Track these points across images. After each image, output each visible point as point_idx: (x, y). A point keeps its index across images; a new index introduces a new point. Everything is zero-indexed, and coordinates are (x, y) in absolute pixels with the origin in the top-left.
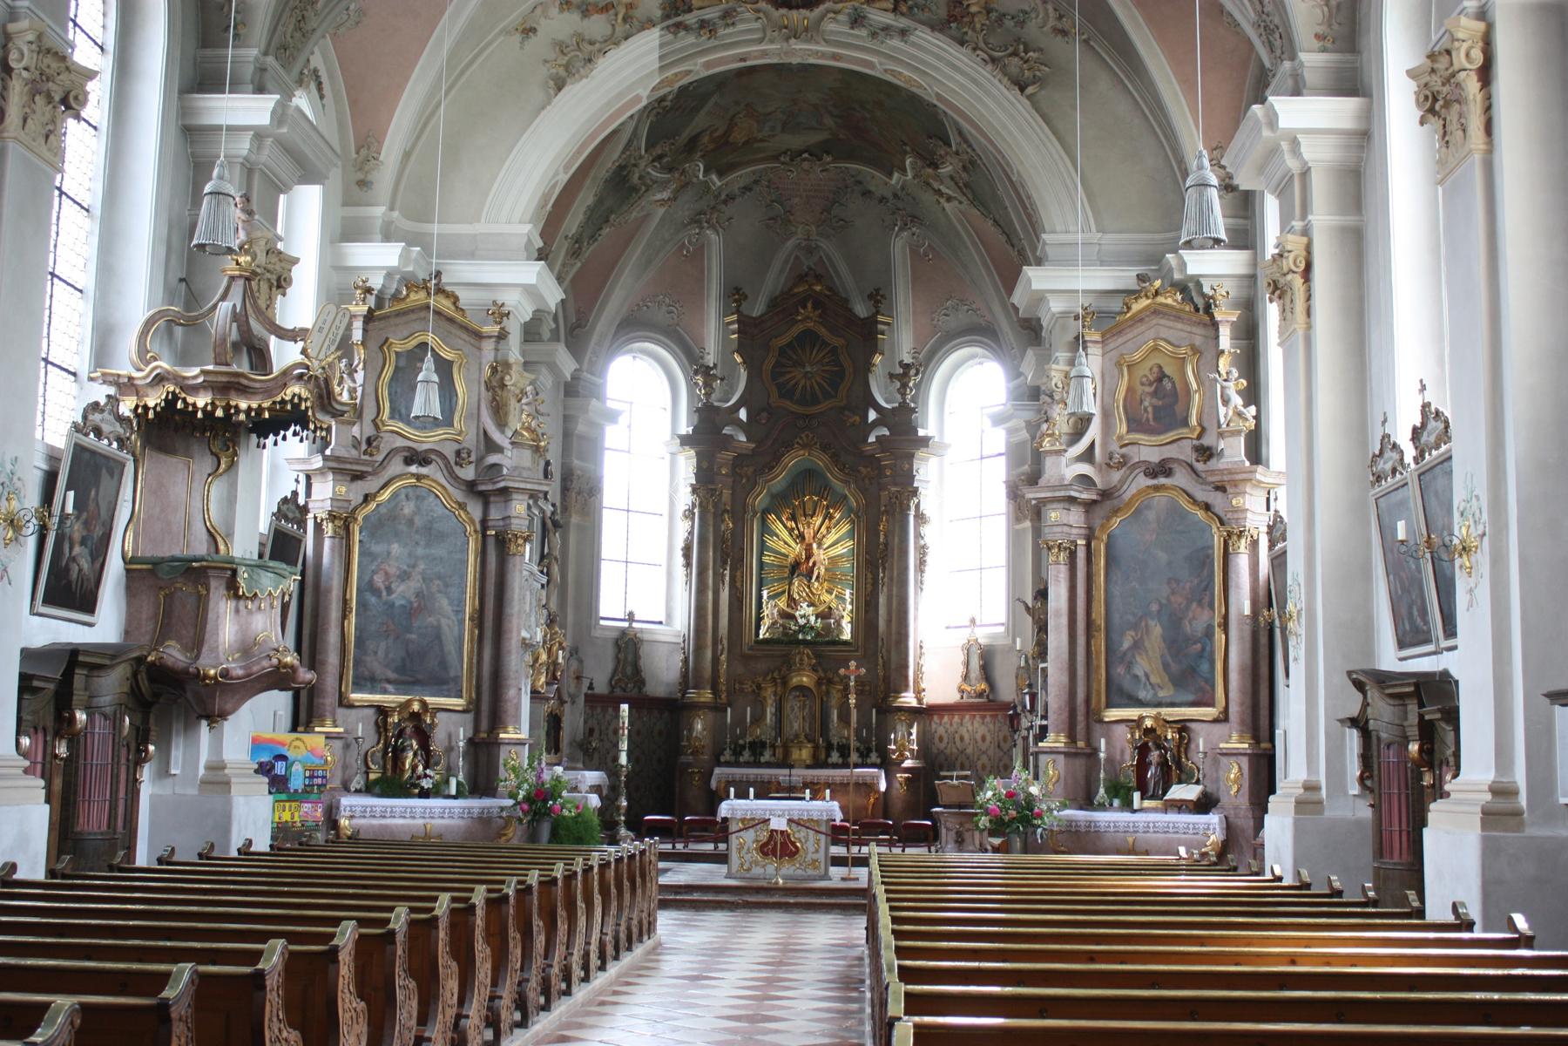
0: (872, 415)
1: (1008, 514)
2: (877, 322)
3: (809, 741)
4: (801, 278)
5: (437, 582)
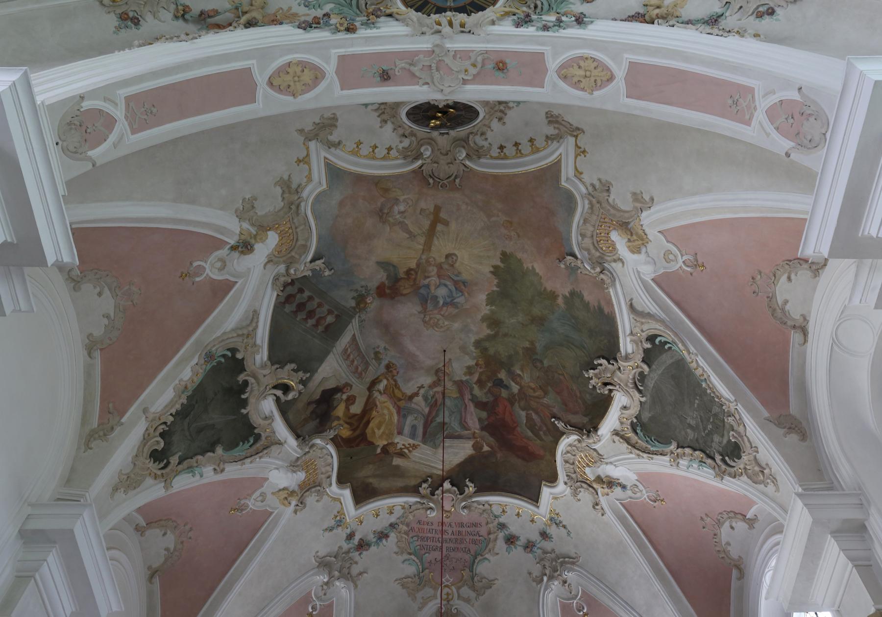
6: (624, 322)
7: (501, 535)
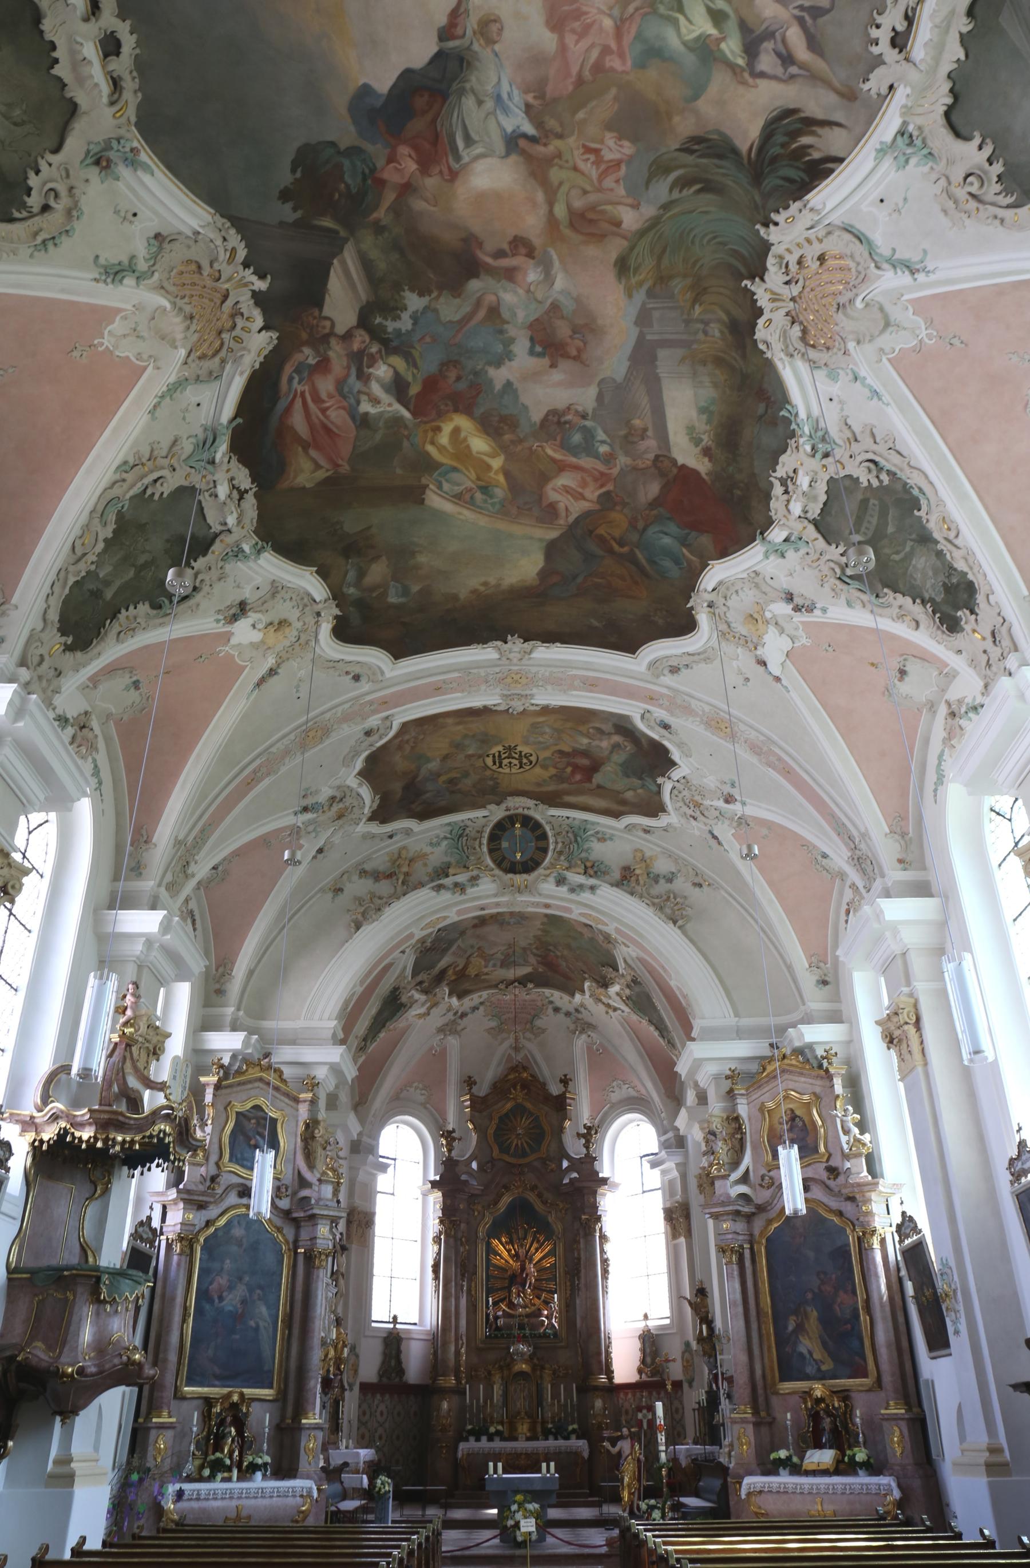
0: (565, 1164)
1: (666, 1233)
2: (566, 1098)
3: (529, 1417)
4: (514, 1069)
5: (258, 1291)
6: (621, 966)
7: (550, 1006)
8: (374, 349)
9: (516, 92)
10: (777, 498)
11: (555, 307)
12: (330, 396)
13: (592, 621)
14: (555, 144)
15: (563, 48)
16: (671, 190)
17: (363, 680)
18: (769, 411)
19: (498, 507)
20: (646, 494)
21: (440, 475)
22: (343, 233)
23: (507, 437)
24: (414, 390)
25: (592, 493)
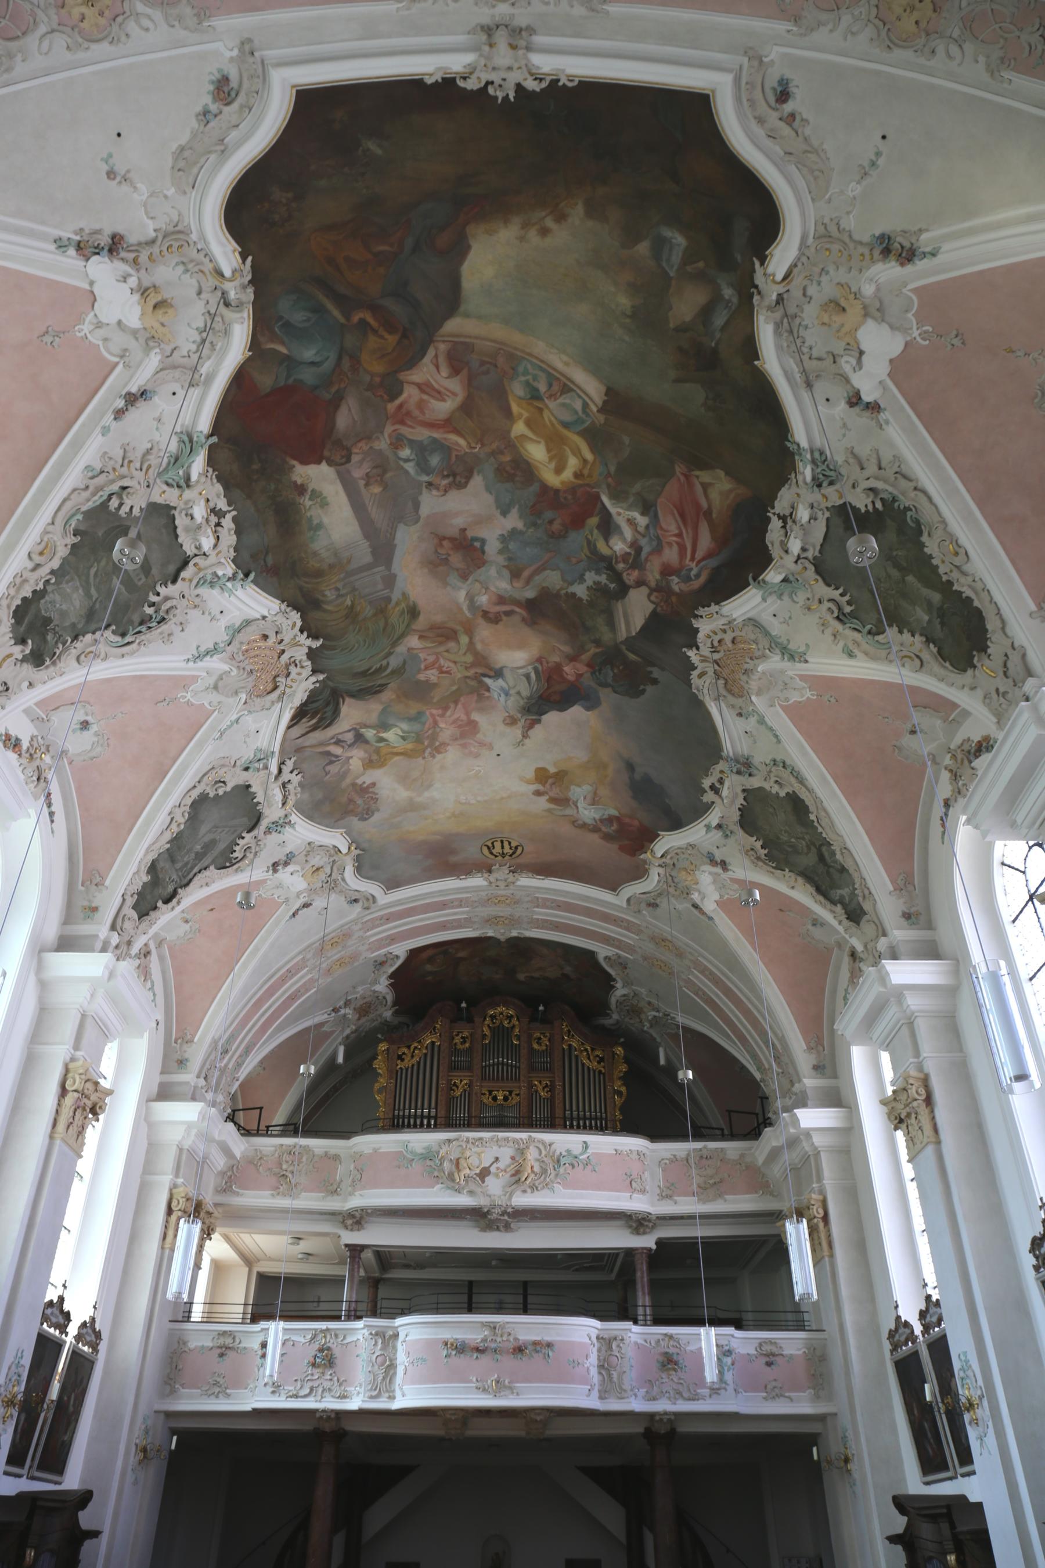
8: (621, 566)
9: (496, 697)
10: (218, 496)
11: (464, 577)
12: (670, 544)
13: (379, 152)
14: (471, 673)
15: (468, 714)
16: (388, 664)
17: (772, 82)
18: (262, 563)
19: (521, 369)
20: (350, 410)
21: (583, 422)
22: (623, 648)
23: (507, 458)
24: (594, 521)
25: (410, 394)
